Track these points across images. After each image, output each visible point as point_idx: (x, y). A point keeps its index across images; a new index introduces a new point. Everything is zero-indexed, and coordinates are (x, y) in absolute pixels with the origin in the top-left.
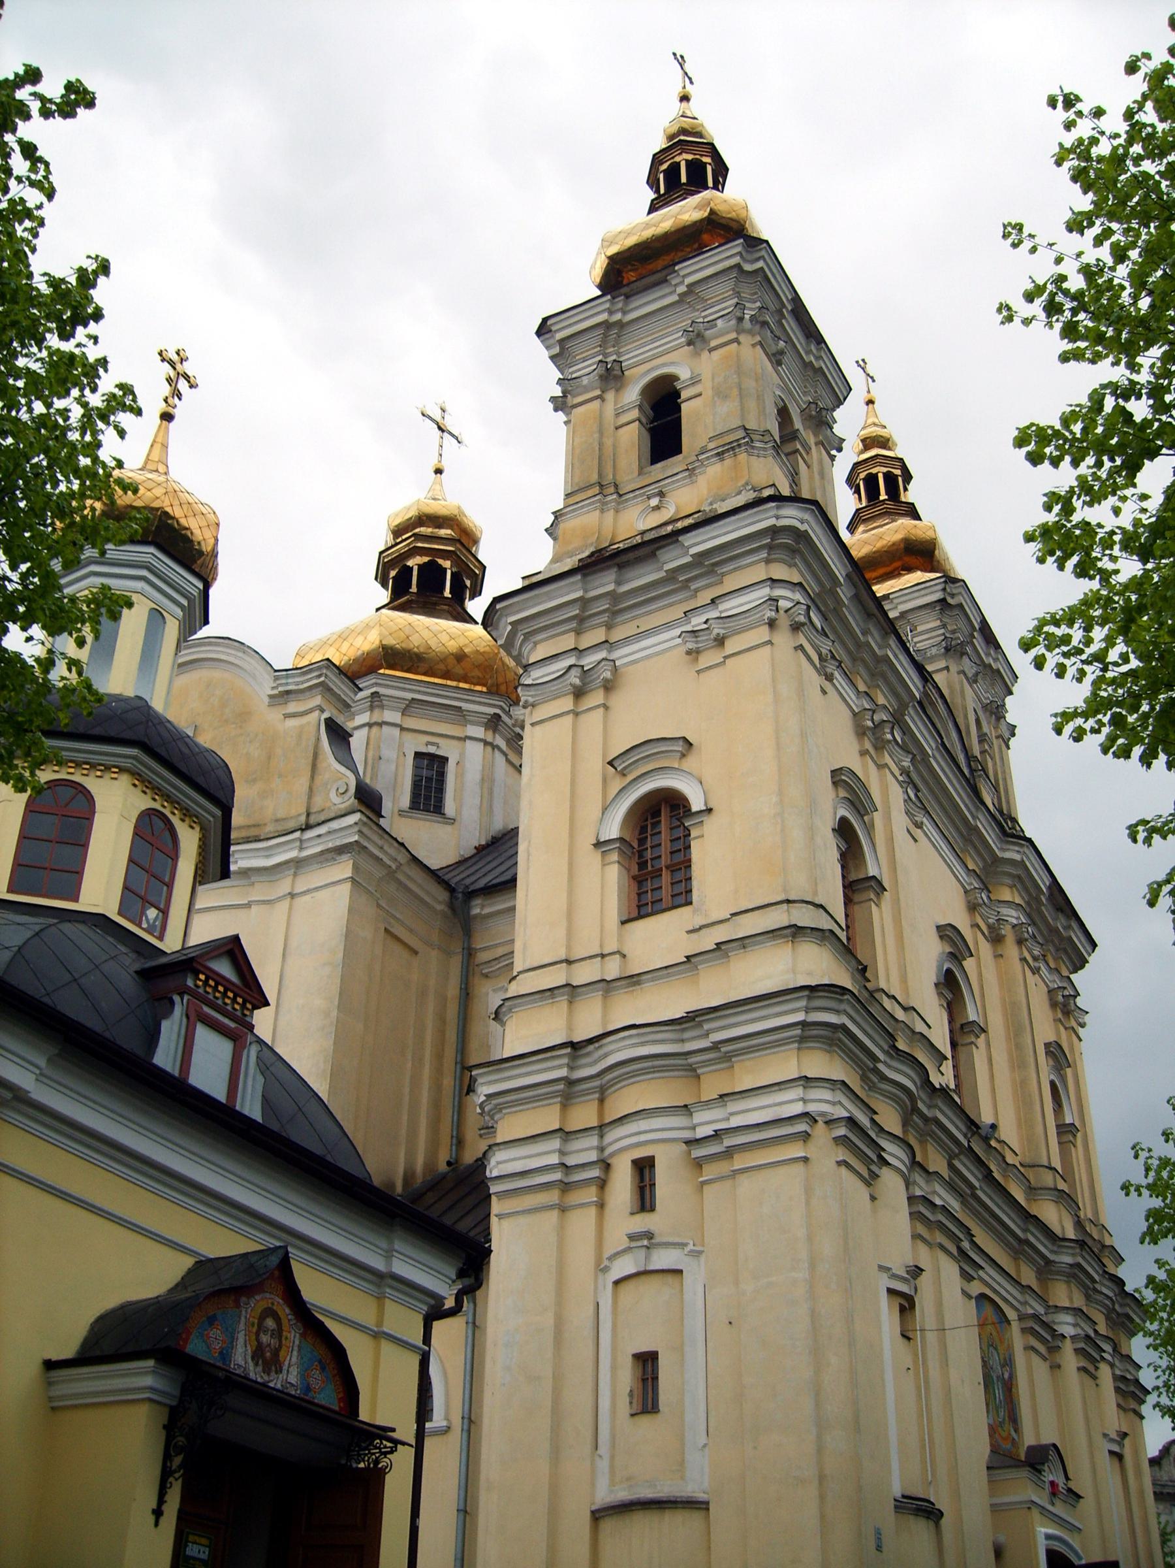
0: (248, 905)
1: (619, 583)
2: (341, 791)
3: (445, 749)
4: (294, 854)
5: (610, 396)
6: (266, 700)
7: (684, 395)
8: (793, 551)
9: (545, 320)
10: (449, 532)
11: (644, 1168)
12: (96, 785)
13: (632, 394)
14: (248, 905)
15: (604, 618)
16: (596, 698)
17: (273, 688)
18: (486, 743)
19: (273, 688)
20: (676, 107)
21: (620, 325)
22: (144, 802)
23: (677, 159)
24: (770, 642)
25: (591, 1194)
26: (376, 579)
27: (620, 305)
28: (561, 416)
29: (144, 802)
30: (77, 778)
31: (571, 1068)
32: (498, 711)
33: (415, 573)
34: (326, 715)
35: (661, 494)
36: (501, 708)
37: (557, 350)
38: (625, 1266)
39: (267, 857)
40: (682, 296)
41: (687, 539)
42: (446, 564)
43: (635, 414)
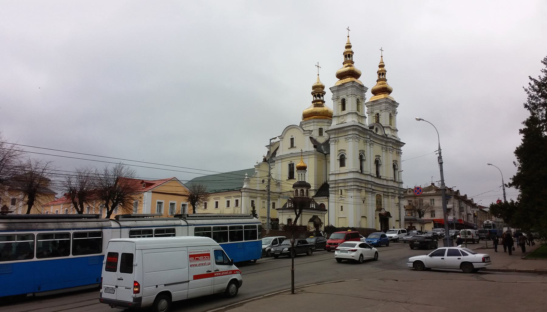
1: (339, 130)
3: (323, 127)
11: (341, 191)
12: (304, 189)
13: (340, 101)
15: (337, 133)
16: (337, 143)
22: (306, 189)
23: (347, 54)
25: (337, 192)
28: (333, 101)
29: (306, 189)
31: (335, 182)
34: (310, 136)
35: (343, 117)
38: (340, 199)
41: (345, 128)
42: (321, 94)
43: (340, 103)
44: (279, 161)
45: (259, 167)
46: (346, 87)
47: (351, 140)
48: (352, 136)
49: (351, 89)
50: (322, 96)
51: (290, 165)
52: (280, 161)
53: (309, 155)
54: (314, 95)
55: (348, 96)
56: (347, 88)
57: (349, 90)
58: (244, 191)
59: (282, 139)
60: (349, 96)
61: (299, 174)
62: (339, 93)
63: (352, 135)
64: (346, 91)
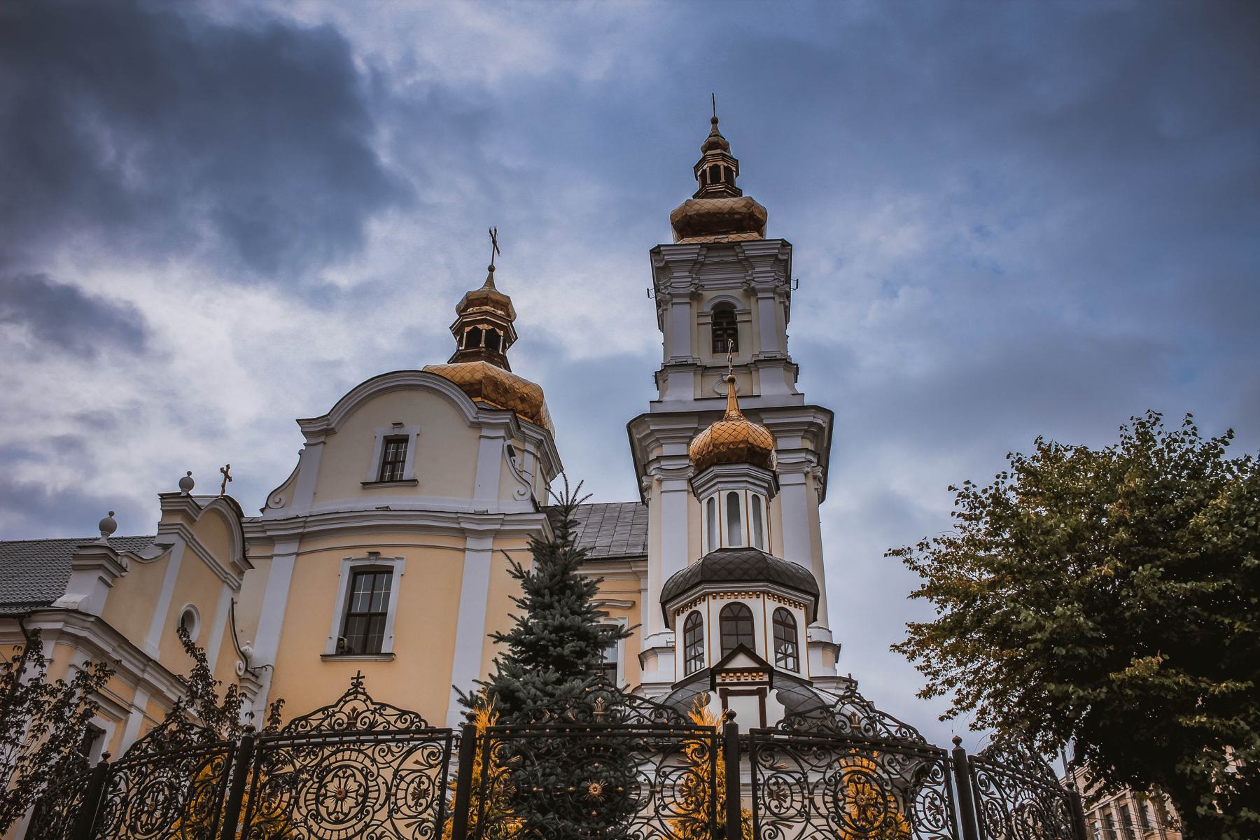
0: (464, 550)
2: (521, 493)
4: (497, 527)
5: (695, 304)
6: (469, 424)
7: (739, 318)
8: (815, 435)
9: (659, 246)
10: (503, 313)
13: (707, 308)
14: (464, 550)
17: (475, 418)
18: (535, 456)
19: (475, 418)
20: (709, 128)
21: (703, 264)
24: (805, 484)
26: (451, 328)
27: (704, 253)
30: (787, 607)
32: (543, 438)
33: (484, 334)
34: (509, 442)
36: (545, 437)
37: (662, 264)
39: (478, 524)
40: (740, 262)
42: (502, 333)
43: (709, 320)
44: (279, 549)
45: (192, 521)
46: (747, 259)
47: (800, 478)
48: (801, 457)
49: (769, 269)
50: (504, 348)
51: (356, 573)
52: (293, 547)
53: (497, 534)
54: (467, 329)
55: (751, 292)
56: (746, 263)
57: (757, 270)
58: (59, 626)
59: (322, 439)
60: (760, 295)
61: (733, 499)
62: (702, 278)
63: (803, 455)
64: (742, 275)
